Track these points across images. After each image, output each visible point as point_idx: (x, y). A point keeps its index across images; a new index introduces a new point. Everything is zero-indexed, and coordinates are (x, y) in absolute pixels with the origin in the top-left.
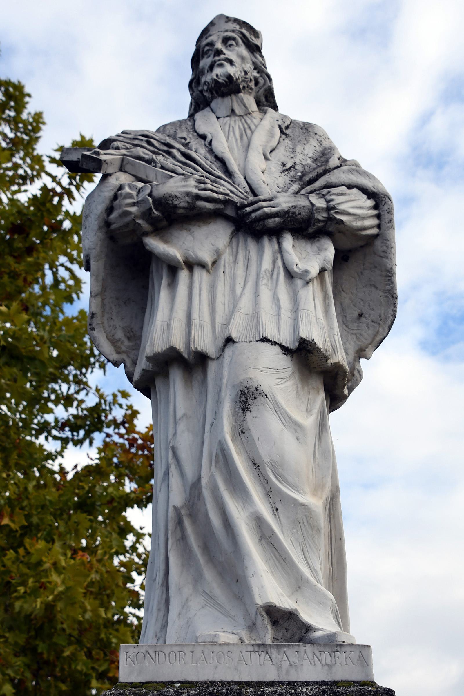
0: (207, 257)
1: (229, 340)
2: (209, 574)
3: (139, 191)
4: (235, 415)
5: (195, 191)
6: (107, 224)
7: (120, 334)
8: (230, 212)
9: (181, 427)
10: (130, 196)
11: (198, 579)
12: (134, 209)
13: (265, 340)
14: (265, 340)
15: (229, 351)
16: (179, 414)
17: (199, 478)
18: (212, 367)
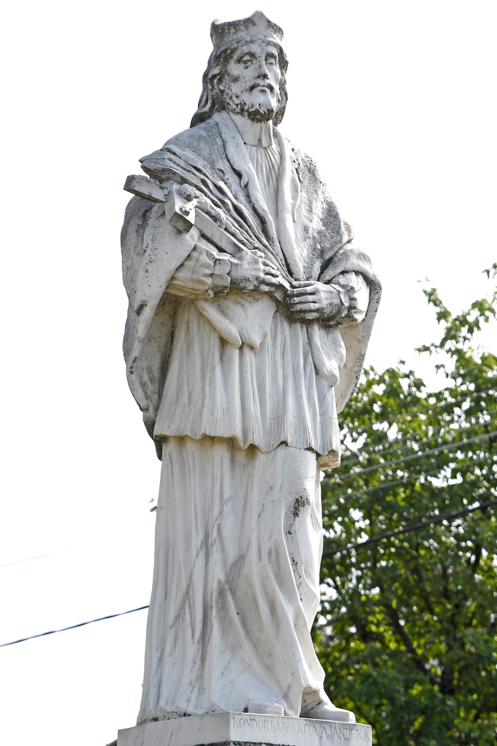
0: (257, 340)
1: (285, 443)
2: (247, 647)
3: (216, 261)
4: (286, 517)
5: (262, 275)
6: (173, 278)
7: (146, 378)
8: (279, 295)
9: (227, 508)
10: (208, 267)
11: (235, 648)
12: (209, 281)
13: (310, 449)
14: (310, 449)
15: (282, 451)
16: (227, 495)
17: (241, 558)
18: (261, 458)
